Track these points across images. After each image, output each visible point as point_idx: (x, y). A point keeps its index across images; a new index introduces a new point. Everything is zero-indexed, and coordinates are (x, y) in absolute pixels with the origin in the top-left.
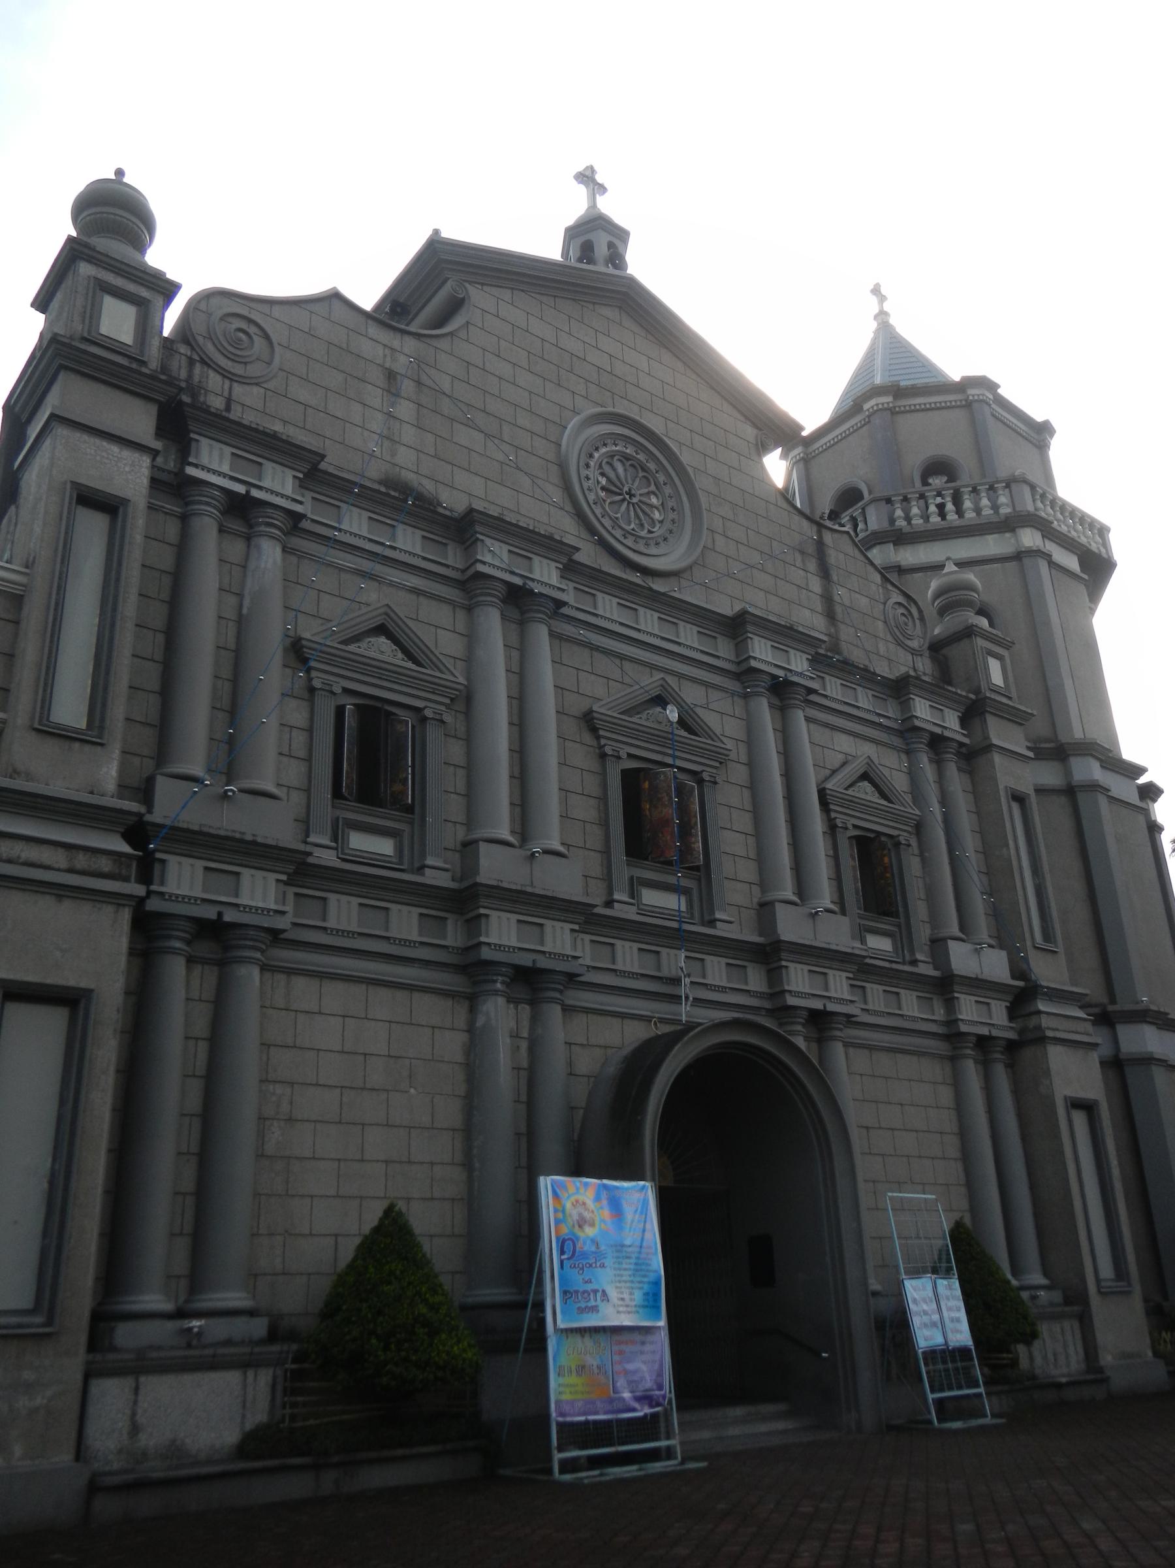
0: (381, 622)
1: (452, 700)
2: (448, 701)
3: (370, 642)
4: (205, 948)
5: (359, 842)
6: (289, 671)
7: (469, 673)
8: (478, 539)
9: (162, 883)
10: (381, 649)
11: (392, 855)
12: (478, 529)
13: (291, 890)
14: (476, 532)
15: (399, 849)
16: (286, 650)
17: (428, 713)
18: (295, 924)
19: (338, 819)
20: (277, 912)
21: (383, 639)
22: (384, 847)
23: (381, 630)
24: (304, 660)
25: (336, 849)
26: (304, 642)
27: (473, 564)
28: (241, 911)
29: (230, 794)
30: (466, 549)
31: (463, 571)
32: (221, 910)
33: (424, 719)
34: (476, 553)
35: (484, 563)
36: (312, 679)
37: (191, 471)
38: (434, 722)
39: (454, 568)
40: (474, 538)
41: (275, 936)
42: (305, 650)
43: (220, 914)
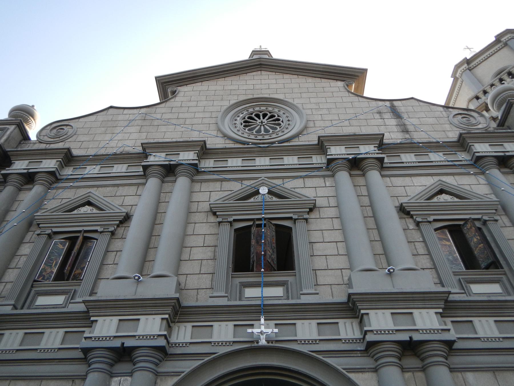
0: (440, 188)
1: (496, 210)
2: (494, 211)
3: (438, 198)
4: (411, 362)
5: (476, 288)
6: (403, 221)
7: (497, 196)
8: (471, 145)
9: (370, 326)
10: (444, 197)
11: (501, 292)
12: (469, 141)
13: (448, 320)
14: (469, 143)
15: (504, 287)
16: (398, 212)
18: (459, 338)
19: (459, 280)
20: (443, 330)
21: (444, 195)
22: (495, 288)
23: (441, 192)
24: (408, 213)
25: (465, 293)
26: (404, 205)
27: (474, 154)
28: (421, 333)
29: (392, 271)
30: (468, 152)
31: (471, 160)
32: (410, 336)
33: (485, 222)
34: (473, 150)
35: (478, 152)
36: (416, 220)
37: (328, 157)
38: (491, 222)
39: (467, 160)
40: (469, 146)
41: (449, 344)
42: (406, 208)
43: (411, 338)
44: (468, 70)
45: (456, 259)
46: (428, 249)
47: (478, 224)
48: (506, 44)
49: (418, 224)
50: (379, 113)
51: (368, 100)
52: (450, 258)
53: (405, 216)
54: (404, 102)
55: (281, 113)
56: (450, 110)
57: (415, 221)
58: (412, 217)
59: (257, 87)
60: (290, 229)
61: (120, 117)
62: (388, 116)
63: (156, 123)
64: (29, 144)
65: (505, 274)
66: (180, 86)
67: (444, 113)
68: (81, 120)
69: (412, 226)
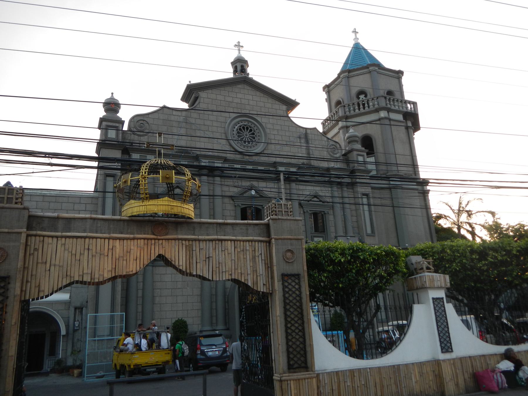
17: (326, 212)
23: (315, 197)
33: (325, 213)
44: (347, 78)
45: (312, 227)
46: (305, 223)
47: (323, 213)
48: (370, 72)
49: (304, 212)
50: (300, 138)
51: (296, 126)
52: (311, 226)
53: (300, 207)
54: (311, 130)
55: (257, 131)
56: (330, 141)
57: (304, 210)
58: (303, 208)
59: (243, 101)
60: (261, 210)
61: (172, 118)
62: (303, 141)
63: (194, 127)
64: (127, 134)
65: (325, 234)
66: (200, 91)
67: (326, 142)
68: (150, 116)
69: (302, 212)
